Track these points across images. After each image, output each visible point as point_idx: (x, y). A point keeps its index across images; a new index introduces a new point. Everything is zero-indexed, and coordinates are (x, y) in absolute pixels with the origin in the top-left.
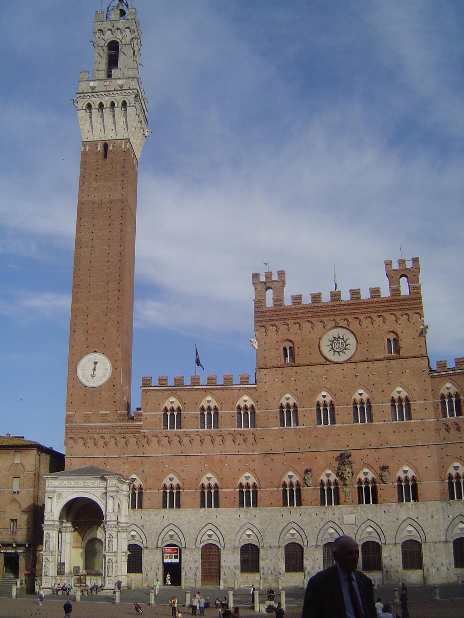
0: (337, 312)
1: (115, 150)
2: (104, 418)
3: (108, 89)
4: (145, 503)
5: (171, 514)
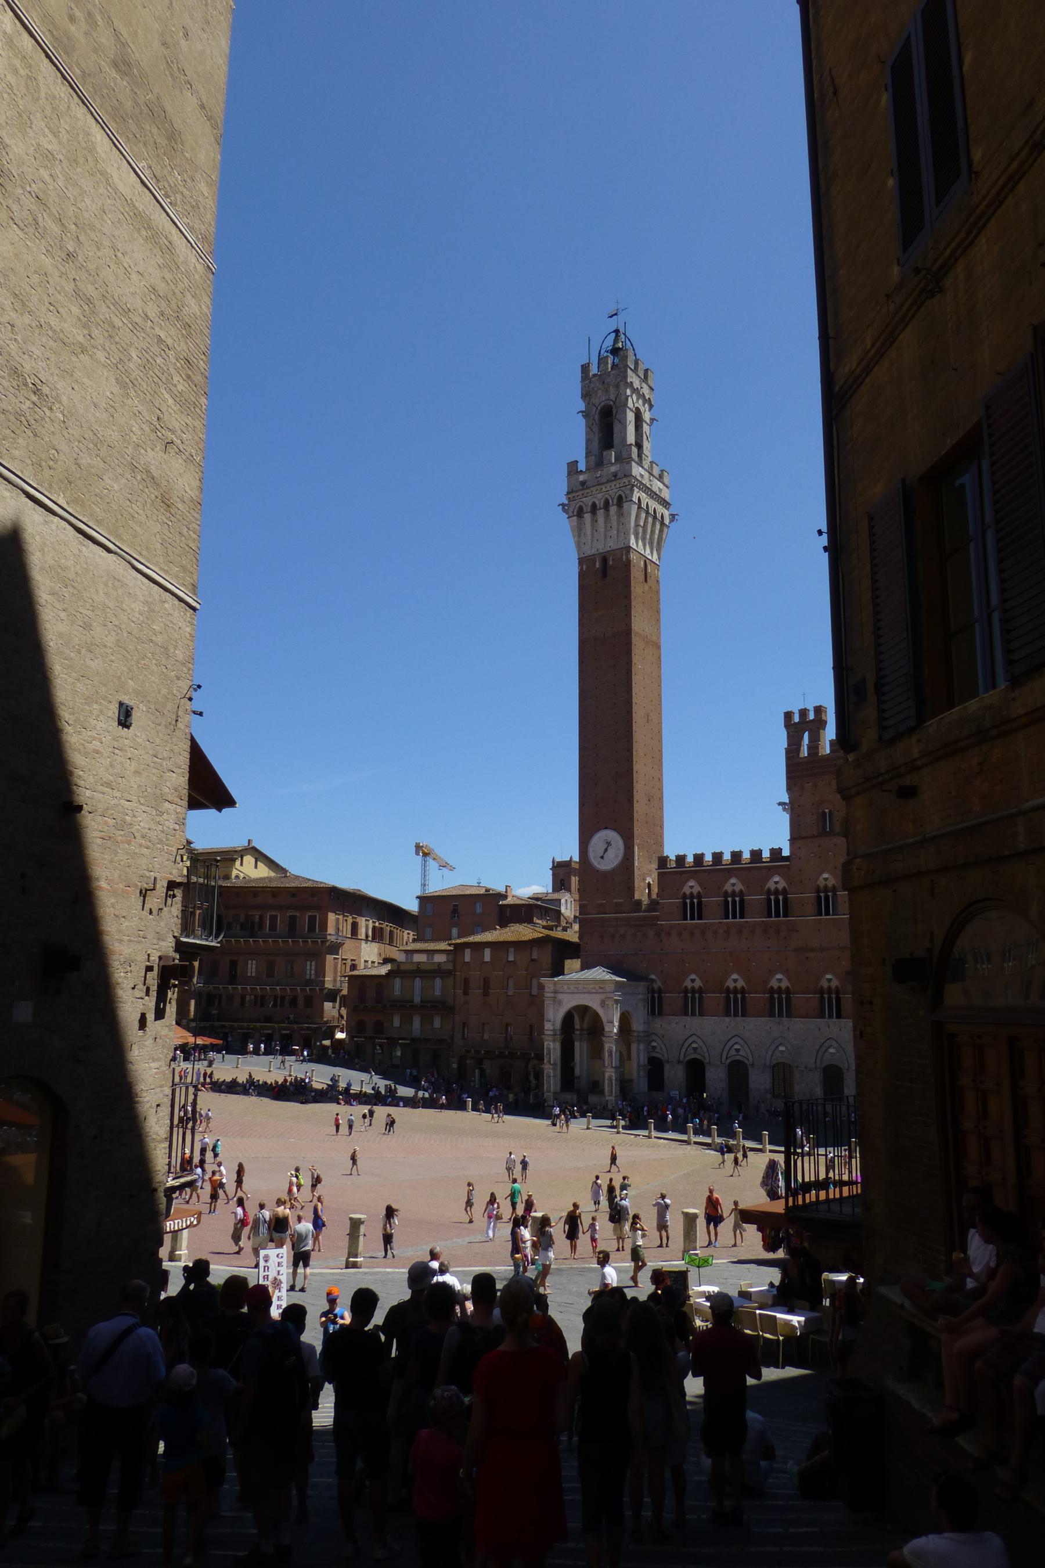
5: (694, 1023)
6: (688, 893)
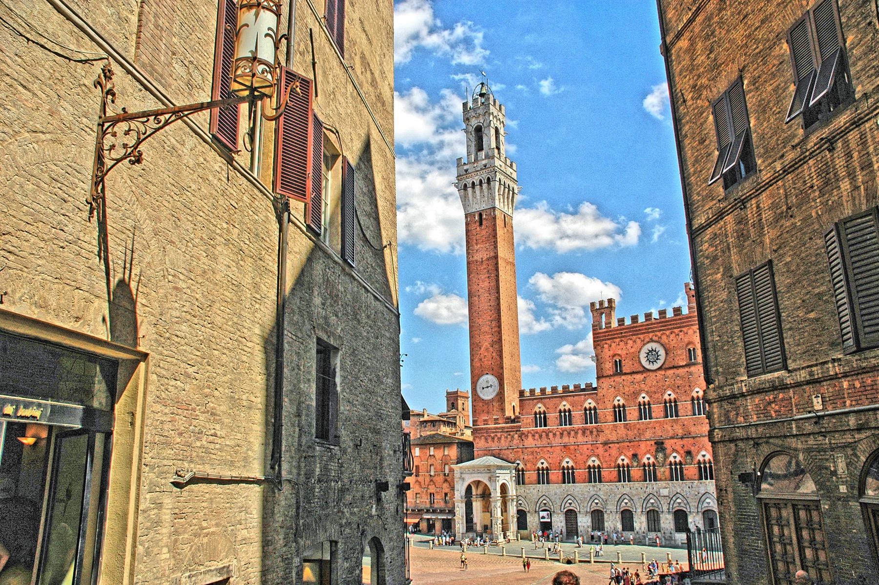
2: (496, 421)
4: (526, 480)
5: (542, 487)
6: (538, 411)
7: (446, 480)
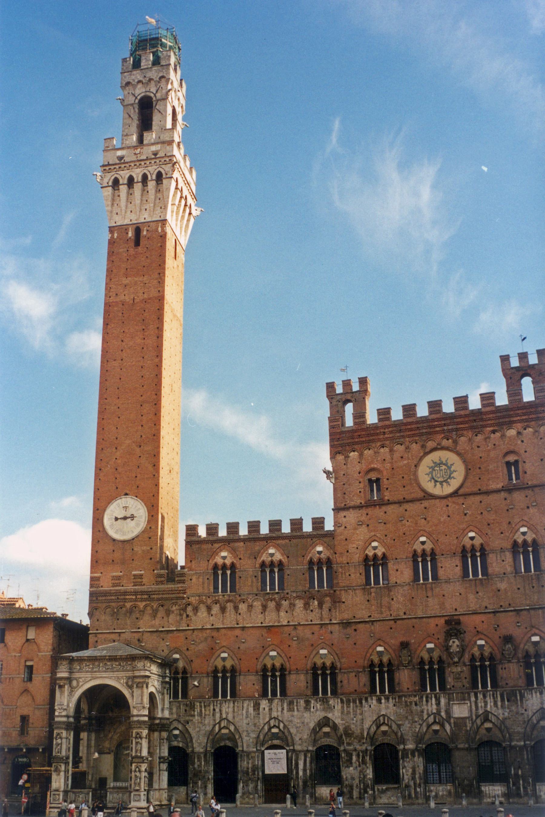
0: (438, 429)
1: (149, 235)
3: (139, 159)
7: (26, 691)
